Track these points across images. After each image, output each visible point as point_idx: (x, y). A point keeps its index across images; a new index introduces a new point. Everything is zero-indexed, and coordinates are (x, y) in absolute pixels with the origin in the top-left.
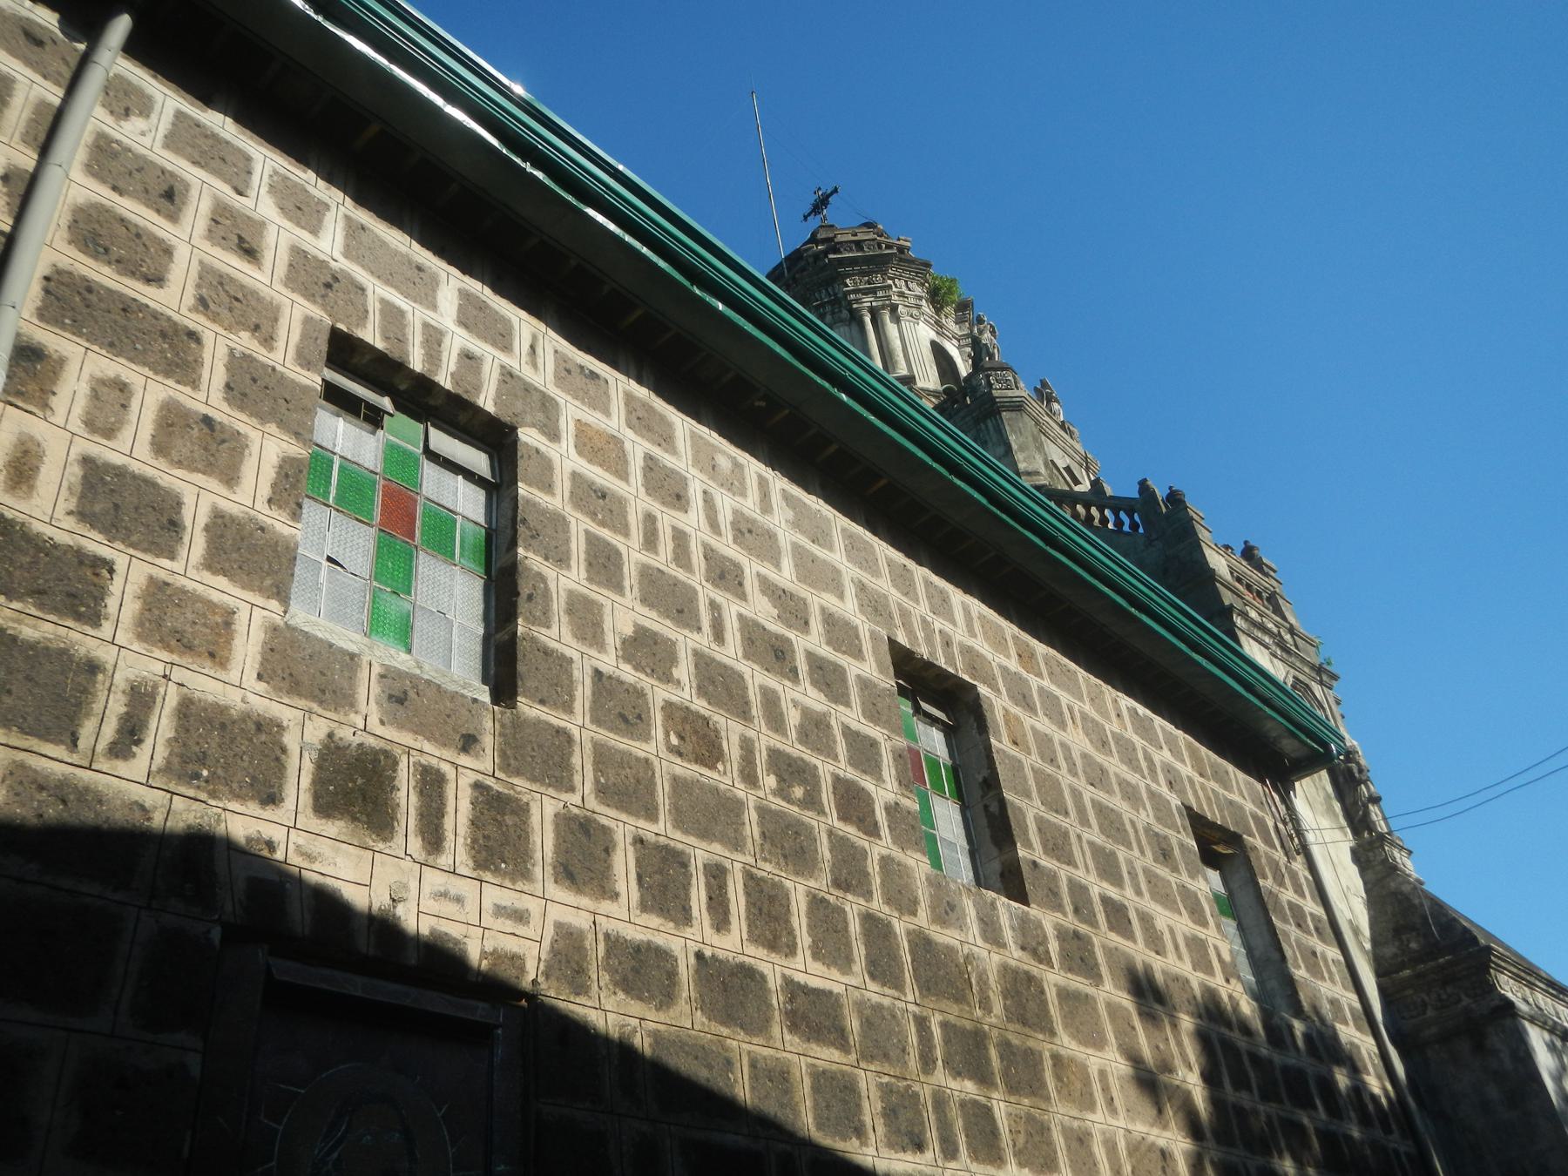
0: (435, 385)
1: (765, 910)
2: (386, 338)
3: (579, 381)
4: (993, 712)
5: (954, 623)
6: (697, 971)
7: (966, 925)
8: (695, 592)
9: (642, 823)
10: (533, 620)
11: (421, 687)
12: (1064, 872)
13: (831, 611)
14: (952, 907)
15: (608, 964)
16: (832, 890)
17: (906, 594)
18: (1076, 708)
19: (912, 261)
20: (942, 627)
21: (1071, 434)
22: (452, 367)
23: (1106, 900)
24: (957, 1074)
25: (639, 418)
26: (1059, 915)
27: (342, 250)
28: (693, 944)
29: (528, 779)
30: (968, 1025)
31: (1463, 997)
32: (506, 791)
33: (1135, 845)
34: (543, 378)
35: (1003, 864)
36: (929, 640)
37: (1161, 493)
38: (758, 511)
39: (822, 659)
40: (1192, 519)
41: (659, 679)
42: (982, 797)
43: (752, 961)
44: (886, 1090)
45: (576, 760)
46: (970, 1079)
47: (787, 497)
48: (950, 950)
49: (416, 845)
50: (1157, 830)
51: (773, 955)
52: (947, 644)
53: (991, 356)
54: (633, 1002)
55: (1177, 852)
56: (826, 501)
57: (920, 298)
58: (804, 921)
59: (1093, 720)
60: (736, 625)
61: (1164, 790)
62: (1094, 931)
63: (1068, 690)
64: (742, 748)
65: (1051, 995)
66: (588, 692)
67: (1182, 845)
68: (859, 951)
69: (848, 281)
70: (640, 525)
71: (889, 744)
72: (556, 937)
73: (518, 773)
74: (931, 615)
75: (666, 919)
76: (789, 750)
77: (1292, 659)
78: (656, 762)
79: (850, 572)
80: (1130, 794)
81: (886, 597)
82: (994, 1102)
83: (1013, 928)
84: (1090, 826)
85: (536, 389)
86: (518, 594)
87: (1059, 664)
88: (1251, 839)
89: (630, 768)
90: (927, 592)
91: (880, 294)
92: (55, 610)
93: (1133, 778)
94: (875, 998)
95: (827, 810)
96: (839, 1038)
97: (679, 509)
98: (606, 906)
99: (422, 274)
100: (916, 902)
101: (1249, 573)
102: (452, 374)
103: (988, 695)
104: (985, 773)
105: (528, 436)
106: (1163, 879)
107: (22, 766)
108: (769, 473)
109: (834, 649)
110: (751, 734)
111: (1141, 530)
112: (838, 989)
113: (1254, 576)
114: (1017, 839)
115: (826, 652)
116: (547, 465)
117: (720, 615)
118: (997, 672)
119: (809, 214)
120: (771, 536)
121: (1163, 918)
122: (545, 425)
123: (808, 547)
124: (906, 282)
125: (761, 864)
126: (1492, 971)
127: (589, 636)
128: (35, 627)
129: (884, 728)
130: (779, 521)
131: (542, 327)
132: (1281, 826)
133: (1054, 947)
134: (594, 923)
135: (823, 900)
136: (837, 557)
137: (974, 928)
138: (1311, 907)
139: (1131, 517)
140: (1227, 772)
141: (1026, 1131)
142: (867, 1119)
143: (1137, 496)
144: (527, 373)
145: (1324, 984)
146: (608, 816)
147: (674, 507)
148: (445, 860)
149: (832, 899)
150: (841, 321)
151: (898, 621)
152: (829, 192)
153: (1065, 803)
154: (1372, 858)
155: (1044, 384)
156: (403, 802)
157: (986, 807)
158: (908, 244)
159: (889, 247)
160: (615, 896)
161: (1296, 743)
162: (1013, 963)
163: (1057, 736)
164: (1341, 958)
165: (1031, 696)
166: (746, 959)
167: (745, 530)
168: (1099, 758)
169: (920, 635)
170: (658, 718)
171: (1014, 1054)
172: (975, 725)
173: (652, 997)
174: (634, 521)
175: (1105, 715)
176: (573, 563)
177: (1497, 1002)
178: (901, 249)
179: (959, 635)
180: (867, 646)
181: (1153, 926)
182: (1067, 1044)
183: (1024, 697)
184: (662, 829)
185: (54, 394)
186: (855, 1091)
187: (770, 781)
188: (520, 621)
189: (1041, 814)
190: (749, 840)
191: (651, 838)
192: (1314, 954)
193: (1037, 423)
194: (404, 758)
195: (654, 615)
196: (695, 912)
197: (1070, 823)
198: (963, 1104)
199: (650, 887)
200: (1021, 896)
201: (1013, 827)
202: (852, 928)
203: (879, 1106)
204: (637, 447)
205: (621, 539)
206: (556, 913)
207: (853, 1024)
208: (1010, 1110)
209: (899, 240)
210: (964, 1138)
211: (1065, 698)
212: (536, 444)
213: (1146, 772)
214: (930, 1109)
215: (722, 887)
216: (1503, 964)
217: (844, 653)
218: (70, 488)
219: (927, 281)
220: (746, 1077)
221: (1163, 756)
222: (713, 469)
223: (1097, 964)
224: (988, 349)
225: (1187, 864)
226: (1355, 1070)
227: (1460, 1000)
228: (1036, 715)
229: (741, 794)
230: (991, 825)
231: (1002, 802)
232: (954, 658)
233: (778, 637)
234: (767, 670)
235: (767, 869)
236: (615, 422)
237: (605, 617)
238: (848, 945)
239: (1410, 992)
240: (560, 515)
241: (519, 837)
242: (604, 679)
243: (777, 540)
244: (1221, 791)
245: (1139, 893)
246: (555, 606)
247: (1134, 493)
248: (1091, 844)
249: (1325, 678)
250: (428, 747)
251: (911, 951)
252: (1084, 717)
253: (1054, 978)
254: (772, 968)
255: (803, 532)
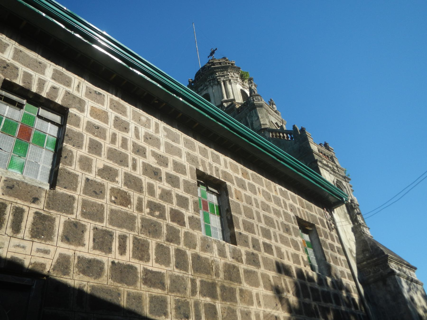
0: (41, 96)
1: (140, 248)
2: (24, 83)
3: (94, 95)
4: (231, 190)
5: (220, 164)
6: (111, 267)
7: (213, 251)
8: (128, 156)
9: (97, 223)
10: (66, 164)
11: (19, 184)
12: (250, 236)
13: (176, 161)
14: (209, 246)
15: (78, 265)
16: (165, 242)
17: (204, 156)
18: (261, 189)
19: (235, 67)
20: (216, 166)
21: (278, 114)
22: (47, 91)
23: (264, 244)
24: (204, 296)
25: (114, 106)
26: (247, 248)
27: (12, 57)
28: (111, 259)
29: (56, 211)
30: (210, 281)
31: (381, 269)
32: (47, 214)
33: (277, 227)
34: (81, 95)
35: (231, 233)
36: (211, 169)
37: (299, 129)
38: (154, 132)
39: (171, 175)
40: (307, 135)
41: (111, 181)
42: (226, 214)
43: (133, 264)
44: (177, 301)
45: (75, 205)
46: (209, 297)
47: (165, 129)
48: (206, 259)
49: (9, 231)
50: (285, 223)
51: (141, 262)
52: (217, 170)
53: (254, 92)
54: (85, 277)
55: (291, 229)
56: (179, 130)
57: (237, 77)
58: (154, 251)
59: (266, 192)
60: (141, 165)
61: (289, 212)
62: (259, 252)
63: (258, 183)
64: (138, 201)
65: (241, 272)
66: (83, 185)
67: (293, 228)
68: (173, 260)
69: (217, 73)
70: (110, 137)
71: (192, 199)
72: (59, 258)
73: (53, 209)
74: (213, 162)
75: (102, 252)
76: (155, 201)
77: (336, 174)
78: (105, 206)
79: (184, 150)
80: (277, 213)
81: (197, 157)
82: (217, 304)
83: (230, 252)
84: (261, 222)
85: (78, 97)
86: (61, 156)
87: (256, 176)
88: (318, 225)
89: (96, 207)
90: (212, 155)
91: (226, 77)
93: (278, 208)
94: (177, 274)
95: (167, 218)
96: (162, 286)
97: (125, 132)
98: (80, 248)
99: (40, 65)
100: (196, 245)
101: (324, 150)
102: (47, 93)
103: (229, 185)
104: (227, 207)
105: (72, 111)
106: (286, 237)
108: (159, 122)
109: (176, 172)
110: (142, 196)
112: (163, 271)
113: (326, 151)
114: (235, 226)
115: (173, 173)
116: (79, 119)
117: (136, 162)
118: (234, 178)
119: (209, 56)
120: (158, 140)
121: (284, 248)
122: (79, 108)
123: (170, 143)
124: (233, 73)
125: (140, 235)
126: (388, 262)
127: (86, 169)
129: (191, 194)
130: (162, 136)
131: (83, 80)
132: (328, 221)
133: (244, 257)
134: (75, 253)
135: (162, 245)
136: (181, 146)
137: (216, 252)
138: (337, 244)
139: (291, 136)
140: (312, 206)
141: (227, 312)
142: (169, 310)
143: (292, 129)
144: (75, 93)
145: (339, 267)
146: (84, 221)
147: (123, 131)
148: (20, 235)
149: (165, 245)
150: (215, 84)
151: (200, 164)
152: (214, 50)
153: (253, 216)
154: (357, 230)
155: (271, 100)
156: (7, 218)
157: (227, 217)
158: (234, 63)
159: (229, 63)
160: (84, 245)
161: (333, 198)
162: (229, 262)
163: (253, 196)
164: (346, 259)
165: (245, 185)
166: (131, 263)
167: (148, 138)
168: (267, 203)
169: (208, 168)
170: (108, 192)
171: (226, 289)
172: (225, 193)
173: (93, 275)
174: (108, 135)
175: (271, 191)
176: (84, 147)
177: (390, 271)
178: (232, 64)
179: (222, 168)
180: (188, 171)
181: (281, 251)
182: (245, 286)
183: (243, 185)
184: (105, 225)
186: (165, 302)
187: (148, 210)
188: (61, 164)
189: (244, 219)
190: (137, 228)
191: (100, 227)
192: (336, 258)
193: (267, 111)
194: (10, 205)
195: (111, 162)
196: (113, 249)
197: (255, 222)
198: (205, 305)
199: (98, 242)
200: (234, 242)
201: (234, 223)
202: (171, 253)
203: (174, 306)
204: (112, 114)
205: (103, 140)
206: (60, 251)
207: (168, 282)
208: (222, 306)
209: (232, 62)
210: (204, 315)
211: (257, 186)
212: (75, 113)
213: (283, 206)
214: (193, 306)
215: (125, 242)
216: (392, 260)
217: (180, 173)
219: (239, 73)
220: (125, 299)
222: (139, 121)
223: (259, 262)
224: (253, 90)
225: (294, 233)
226: (348, 291)
227: (379, 271)
228: (246, 190)
229: (136, 214)
230: (228, 223)
231: (231, 216)
232: (219, 174)
233: (156, 168)
234: (151, 178)
235: (142, 236)
236: (106, 107)
237: (93, 163)
238: (169, 258)
239: (366, 268)
240: (81, 133)
241: (50, 228)
242: (89, 181)
243: (160, 141)
244: (309, 212)
245: (276, 241)
246: (75, 160)
247: (291, 129)
248: (261, 227)
249: (346, 180)
250: (19, 201)
251: (192, 260)
252: (263, 191)
253: (243, 267)
254: (140, 266)
255: (169, 139)
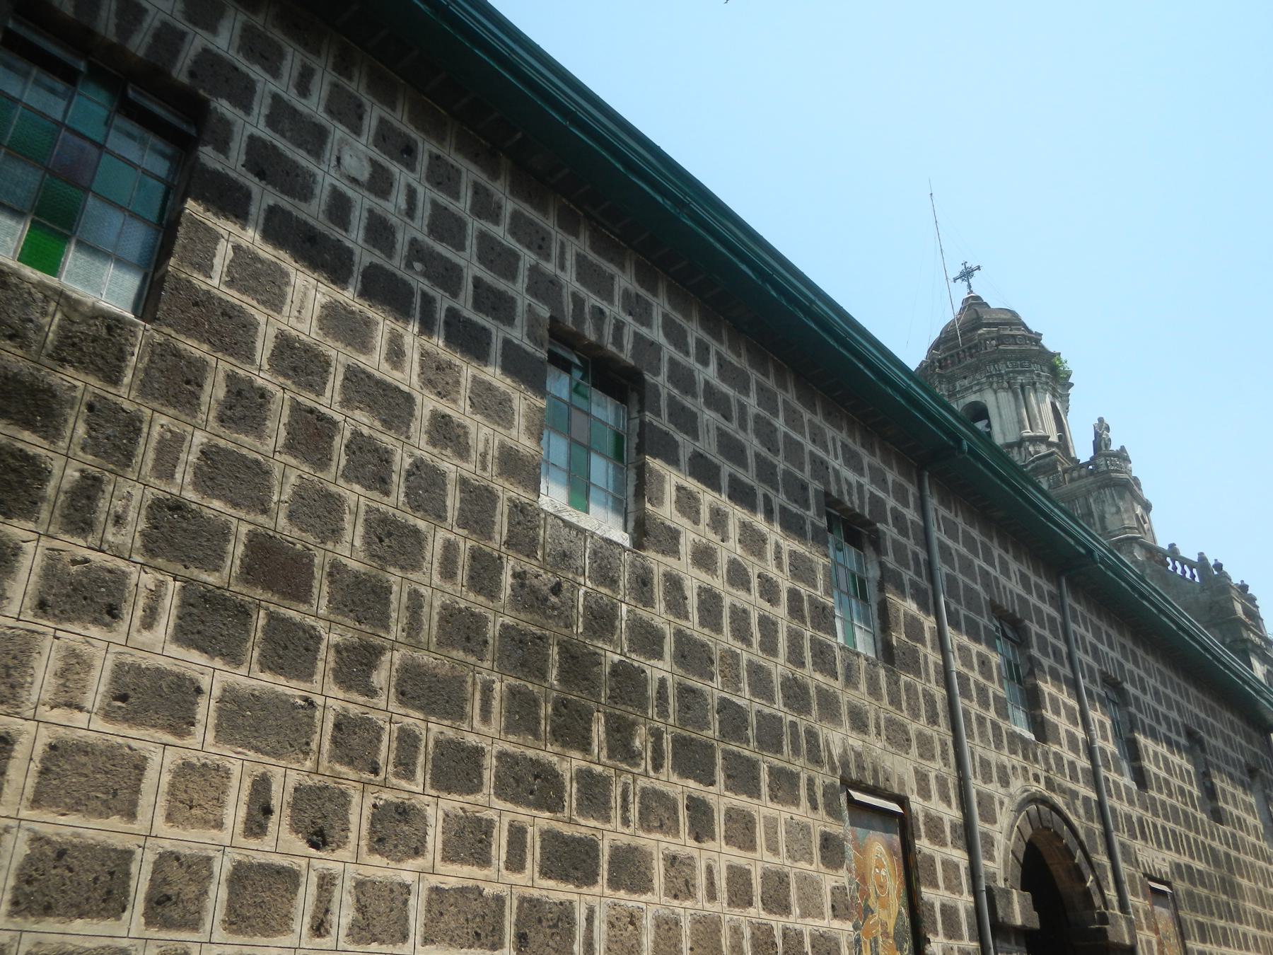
37: (1212, 563)
111: (1197, 579)
221: (1238, 739)
231: (1212, 784)
247: (1195, 558)
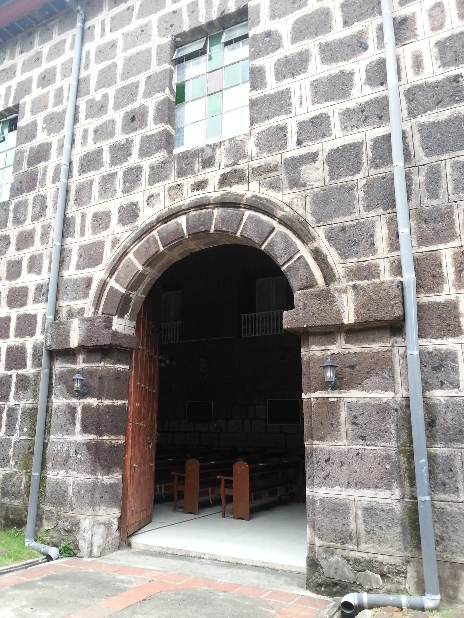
92: (448, 104)
107: (457, 162)
128: (443, 115)
185: (416, 29)
218: (436, 58)
